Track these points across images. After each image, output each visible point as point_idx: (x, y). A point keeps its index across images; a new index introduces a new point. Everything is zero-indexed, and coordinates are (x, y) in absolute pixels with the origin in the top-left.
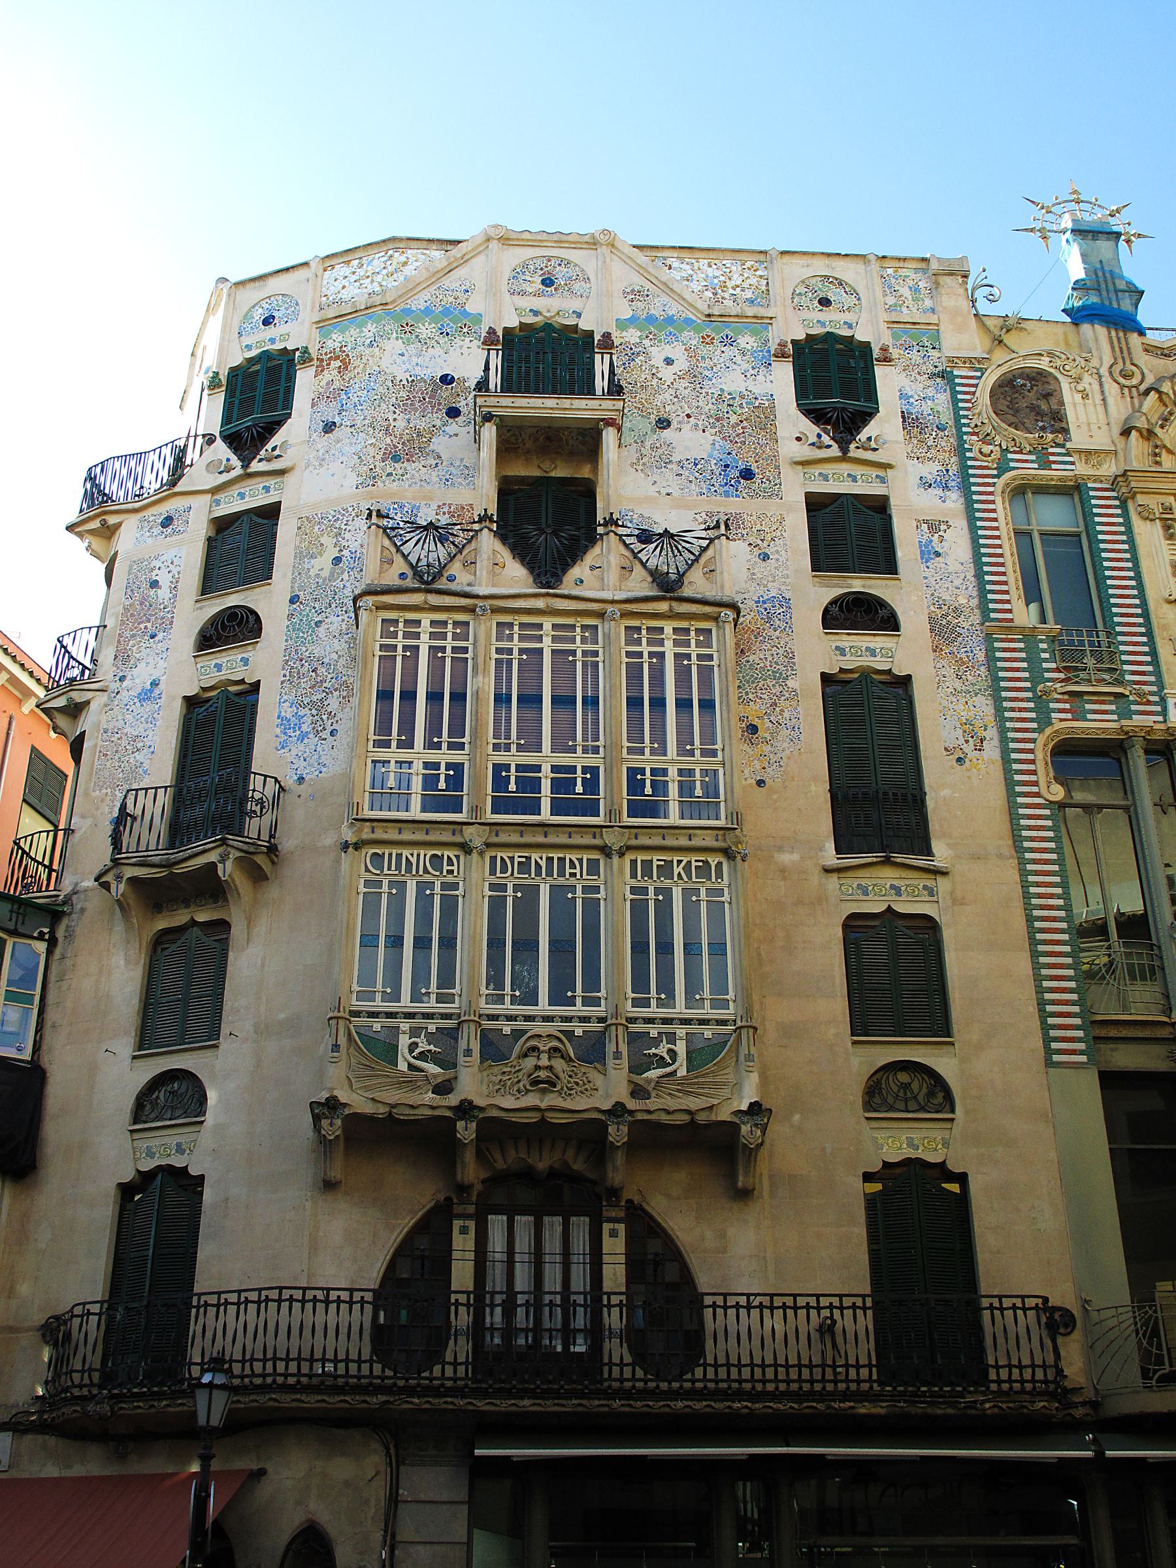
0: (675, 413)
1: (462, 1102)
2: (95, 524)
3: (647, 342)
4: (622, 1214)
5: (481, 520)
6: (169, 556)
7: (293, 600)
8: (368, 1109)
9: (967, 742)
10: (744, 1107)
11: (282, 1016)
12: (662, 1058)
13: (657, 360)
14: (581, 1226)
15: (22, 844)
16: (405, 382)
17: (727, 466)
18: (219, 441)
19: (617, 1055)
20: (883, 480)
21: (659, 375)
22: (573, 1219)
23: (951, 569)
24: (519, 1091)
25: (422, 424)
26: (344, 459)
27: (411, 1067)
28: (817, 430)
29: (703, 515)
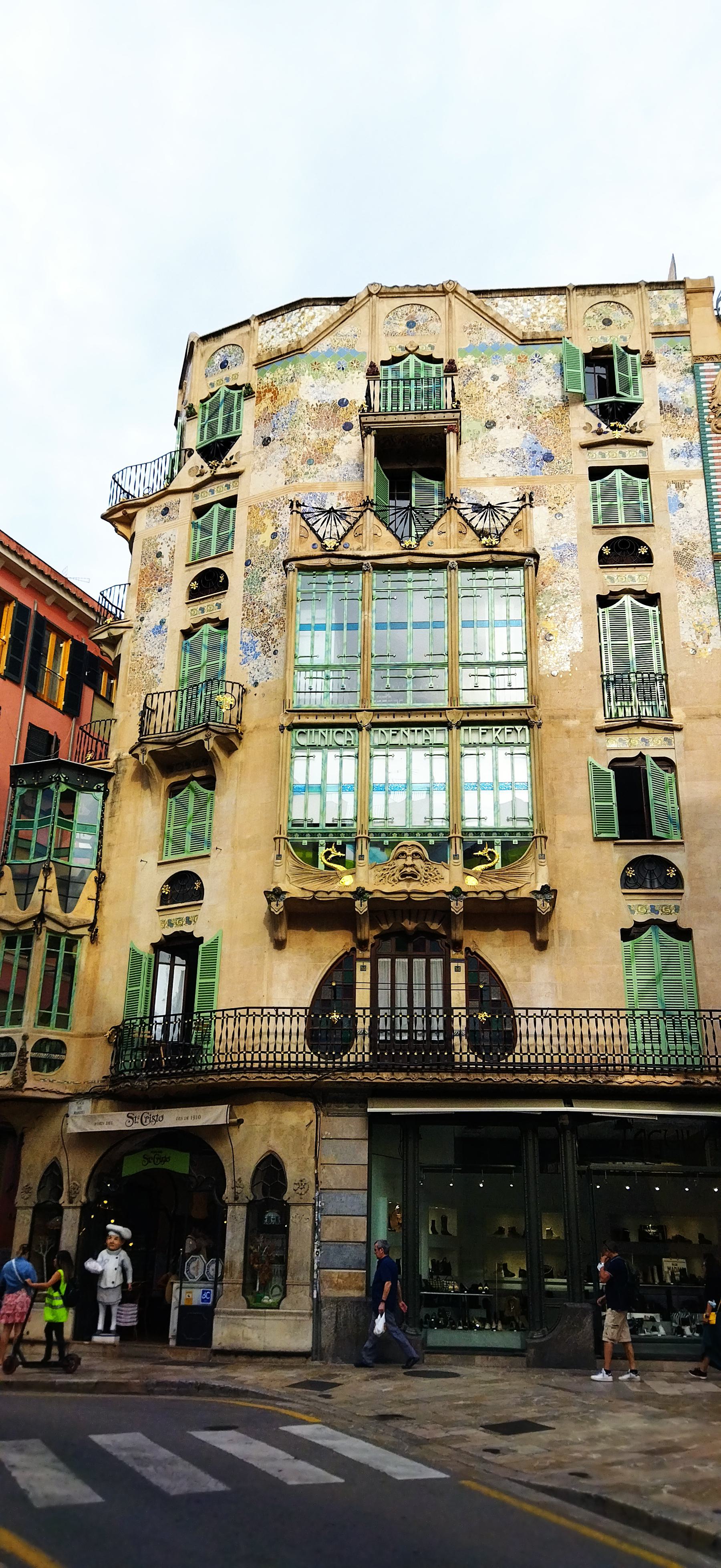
0: (499, 416)
1: (358, 888)
3: (479, 365)
4: (463, 957)
5: (365, 504)
6: (167, 535)
7: (247, 563)
8: (299, 894)
9: (698, 637)
10: (539, 889)
11: (248, 836)
12: (486, 857)
13: (487, 378)
14: (437, 963)
15: (85, 728)
16: (315, 406)
17: (534, 452)
18: (195, 453)
19: (456, 856)
20: (644, 454)
21: (488, 389)
22: (432, 960)
23: (691, 515)
24: (394, 880)
25: (327, 436)
26: (277, 463)
27: (327, 867)
28: (598, 421)
29: (518, 489)
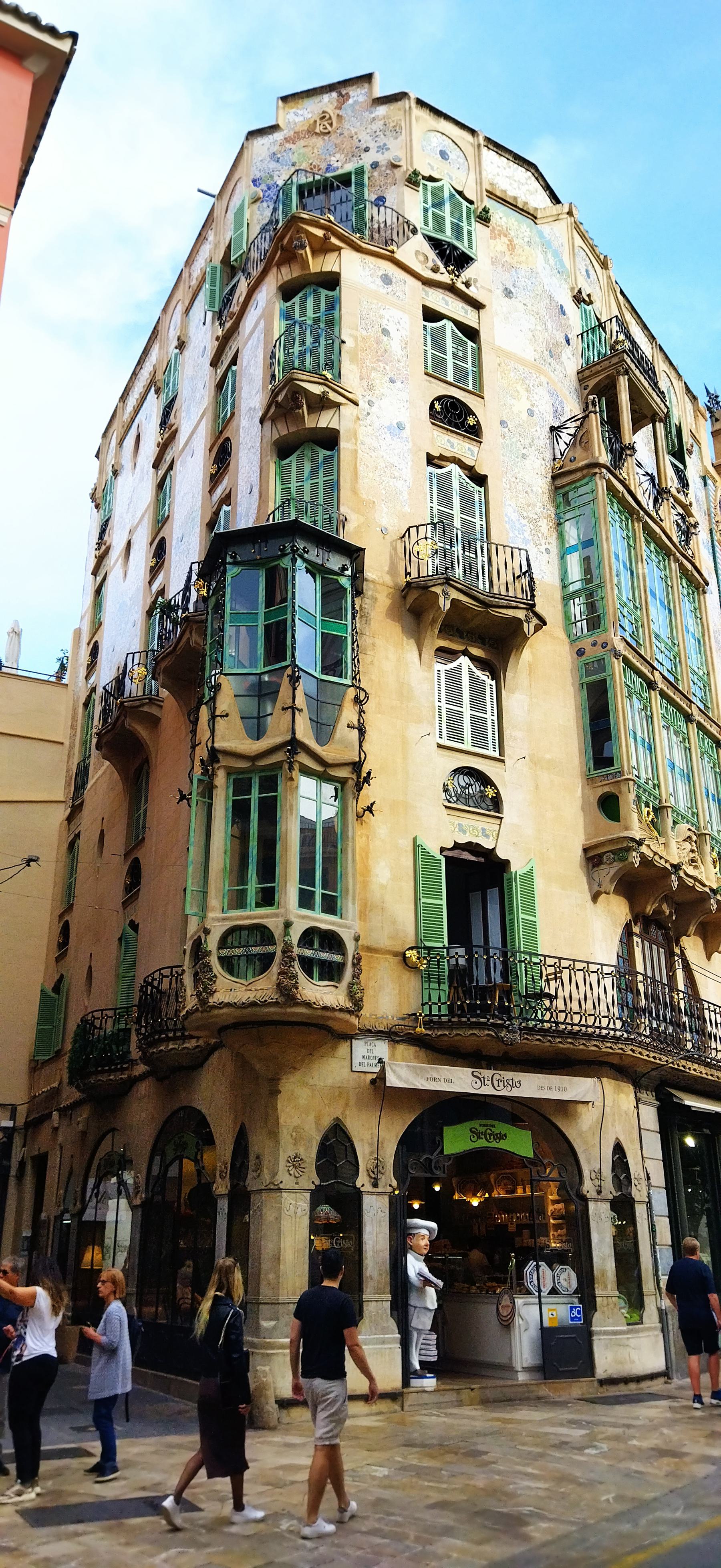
2: (320, 233)
11: (548, 756)
